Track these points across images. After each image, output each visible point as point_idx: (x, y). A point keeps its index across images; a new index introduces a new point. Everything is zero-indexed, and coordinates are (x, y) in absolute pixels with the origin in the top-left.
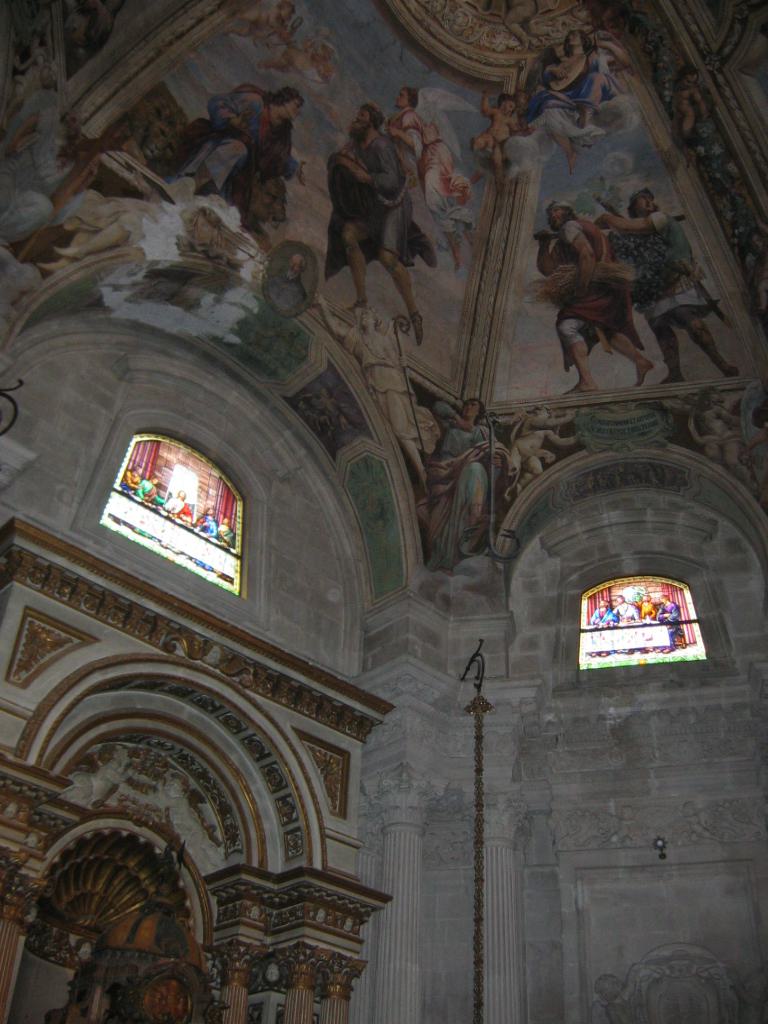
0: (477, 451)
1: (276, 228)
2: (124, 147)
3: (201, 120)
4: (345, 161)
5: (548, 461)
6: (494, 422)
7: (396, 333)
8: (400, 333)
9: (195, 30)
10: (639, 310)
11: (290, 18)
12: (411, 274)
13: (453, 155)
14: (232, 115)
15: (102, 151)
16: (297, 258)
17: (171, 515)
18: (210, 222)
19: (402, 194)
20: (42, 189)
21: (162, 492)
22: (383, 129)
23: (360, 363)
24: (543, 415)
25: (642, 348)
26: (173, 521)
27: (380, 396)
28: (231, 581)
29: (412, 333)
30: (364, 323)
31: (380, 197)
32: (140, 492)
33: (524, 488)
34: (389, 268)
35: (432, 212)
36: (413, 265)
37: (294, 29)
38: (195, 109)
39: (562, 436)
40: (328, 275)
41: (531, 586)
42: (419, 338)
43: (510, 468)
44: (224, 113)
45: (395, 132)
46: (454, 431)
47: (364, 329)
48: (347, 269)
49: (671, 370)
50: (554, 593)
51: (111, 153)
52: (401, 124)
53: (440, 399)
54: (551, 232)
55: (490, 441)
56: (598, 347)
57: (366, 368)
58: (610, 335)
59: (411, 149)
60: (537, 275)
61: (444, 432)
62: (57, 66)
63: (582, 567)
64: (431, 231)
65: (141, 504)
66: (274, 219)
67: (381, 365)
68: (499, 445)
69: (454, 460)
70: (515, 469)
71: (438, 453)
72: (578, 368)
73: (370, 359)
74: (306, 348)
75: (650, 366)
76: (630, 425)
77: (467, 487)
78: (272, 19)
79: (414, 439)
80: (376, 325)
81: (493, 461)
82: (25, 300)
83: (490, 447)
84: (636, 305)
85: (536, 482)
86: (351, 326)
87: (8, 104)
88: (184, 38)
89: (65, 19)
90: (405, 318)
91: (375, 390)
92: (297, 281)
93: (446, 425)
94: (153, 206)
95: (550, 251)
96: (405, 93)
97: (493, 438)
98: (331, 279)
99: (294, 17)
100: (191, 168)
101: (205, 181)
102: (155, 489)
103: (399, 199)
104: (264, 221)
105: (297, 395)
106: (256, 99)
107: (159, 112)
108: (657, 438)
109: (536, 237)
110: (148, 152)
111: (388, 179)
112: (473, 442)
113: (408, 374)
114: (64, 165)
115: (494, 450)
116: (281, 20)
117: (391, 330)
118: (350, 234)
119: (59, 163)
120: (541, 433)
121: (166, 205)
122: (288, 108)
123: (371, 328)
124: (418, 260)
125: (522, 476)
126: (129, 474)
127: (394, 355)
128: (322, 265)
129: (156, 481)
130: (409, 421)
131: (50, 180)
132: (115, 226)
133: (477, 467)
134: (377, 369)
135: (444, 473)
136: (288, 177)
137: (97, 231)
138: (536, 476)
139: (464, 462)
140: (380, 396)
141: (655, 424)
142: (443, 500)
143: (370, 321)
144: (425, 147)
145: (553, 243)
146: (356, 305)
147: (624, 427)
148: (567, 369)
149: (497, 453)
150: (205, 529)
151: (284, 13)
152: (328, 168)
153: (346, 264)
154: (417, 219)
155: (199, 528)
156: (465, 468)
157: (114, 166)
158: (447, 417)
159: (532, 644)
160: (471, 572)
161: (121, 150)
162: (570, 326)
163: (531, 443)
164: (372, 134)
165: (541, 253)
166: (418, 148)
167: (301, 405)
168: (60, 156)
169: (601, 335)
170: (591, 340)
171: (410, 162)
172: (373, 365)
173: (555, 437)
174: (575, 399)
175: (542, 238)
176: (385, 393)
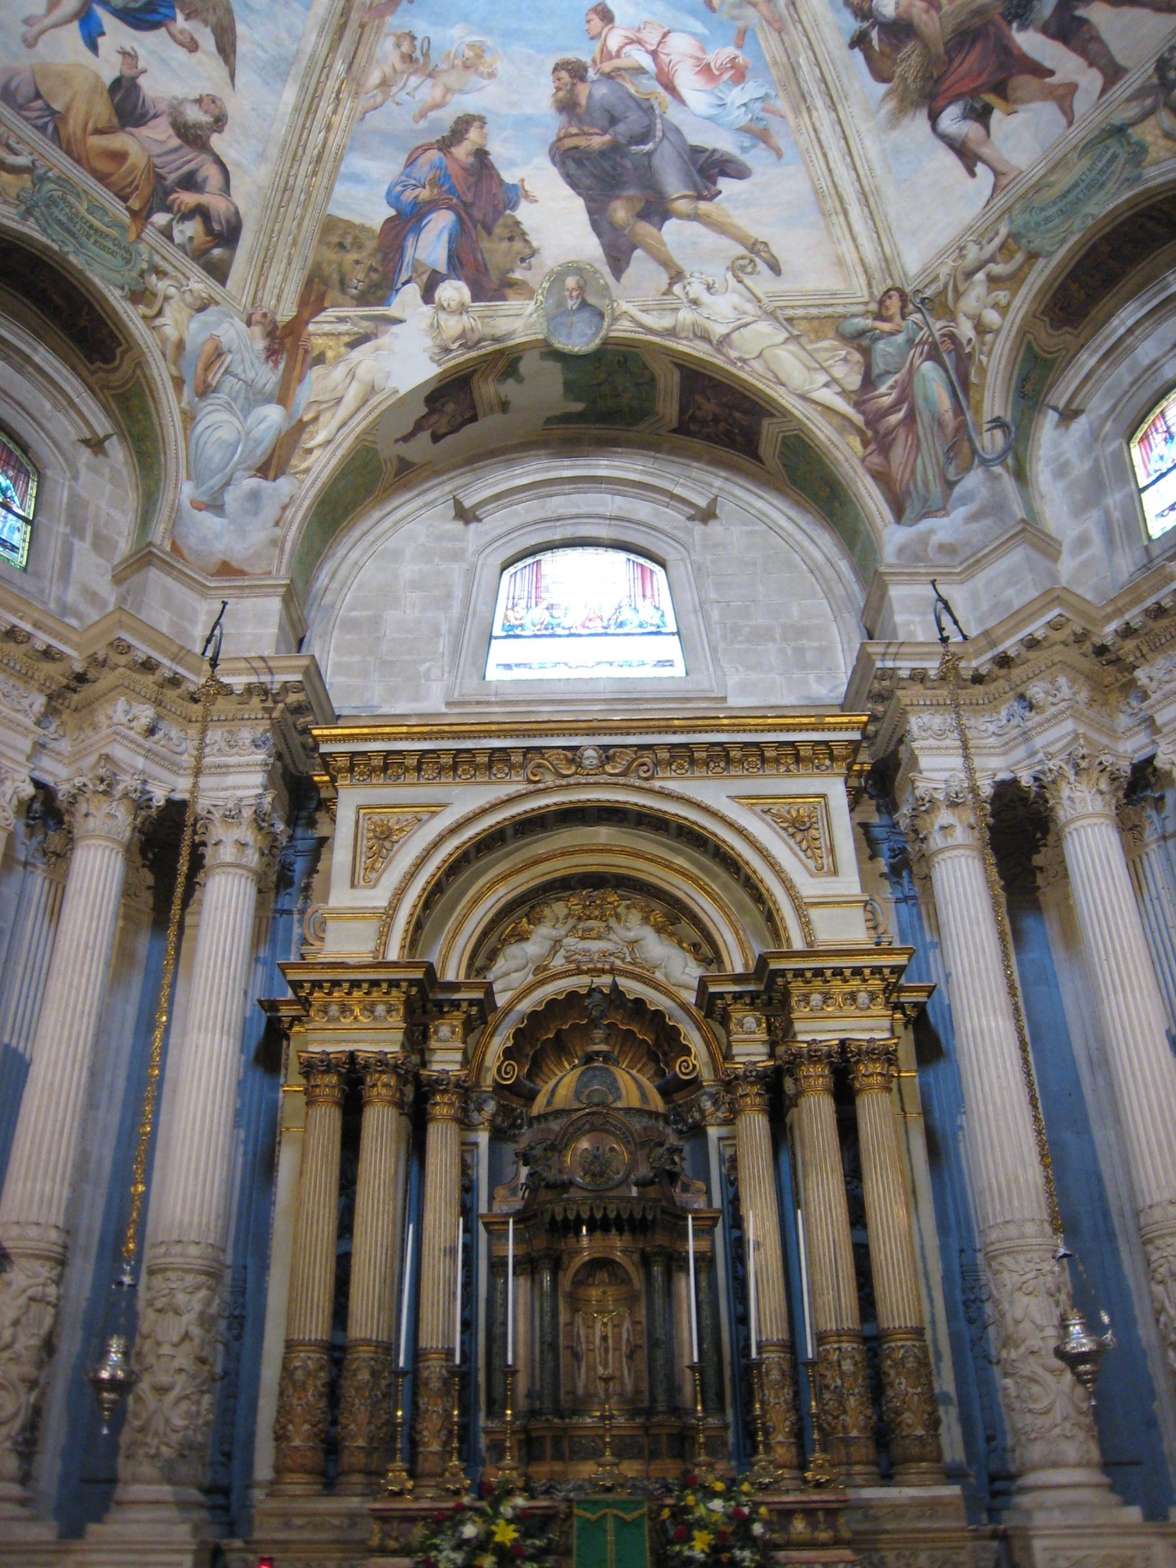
0: (919, 349)
1: (529, 268)
2: (326, 304)
3: (389, 221)
4: (569, 143)
5: (1003, 302)
6: (923, 300)
7: (740, 282)
8: (748, 281)
9: (330, 142)
10: (1023, 27)
11: (414, 47)
12: (726, 205)
13: (694, 35)
14: (417, 191)
15: (307, 323)
16: (571, 282)
17: (573, 631)
18: (453, 312)
19: (659, 126)
20: (268, 400)
21: (555, 613)
22: (591, 74)
23: (709, 341)
24: (973, 254)
25: (1051, 73)
26: (580, 635)
27: (754, 363)
28: (670, 663)
29: (761, 266)
30: (691, 296)
31: (634, 148)
32: (528, 625)
33: (989, 355)
34: (695, 217)
35: (709, 118)
36: (720, 192)
37: (426, 55)
38: (377, 214)
39: (1006, 262)
40: (618, 279)
41: (1061, 471)
42: (775, 267)
43: (964, 342)
44: (409, 195)
45: (607, 67)
46: (880, 345)
47: (695, 302)
48: (638, 253)
49: (1102, 70)
50: (1087, 465)
51: (317, 319)
52: (609, 53)
53: (844, 317)
54: (866, 25)
55: (928, 324)
56: (997, 116)
57: (720, 343)
58: (1000, 89)
59: (640, 71)
60: (882, 88)
61: (866, 352)
62: (199, 284)
63: (1114, 407)
64: (724, 143)
65: (535, 636)
66: (523, 260)
67: (739, 328)
68: (939, 324)
69: (897, 376)
70: (970, 340)
71: (869, 381)
72: (984, 162)
73: (719, 330)
74: (645, 367)
75: (1073, 88)
76: (1083, 185)
77: (926, 399)
78: (399, 66)
79: (826, 385)
80: (709, 288)
81: (942, 348)
82: (289, 513)
83: (931, 334)
84: (1015, 25)
85: (1002, 337)
86: (678, 309)
87: (164, 355)
88: (325, 157)
89: (170, 238)
90: (742, 258)
91: (744, 361)
92: (584, 305)
93: (865, 342)
94: (383, 340)
95: (877, 48)
96: (593, 16)
97: (930, 320)
98: (625, 278)
99: (418, 43)
100: (404, 277)
101: (425, 277)
102: (547, 613)
103: (659, 134)
104: (512, 270)
105: (680, 420)
106: (434, 155)
107: (341, 246)
108: (1125, 175)
109: (853, 45)
110: (354, 292)
111: (633, 122)
112: (910, 342)
113: (781, 317)
114: (276, 363)
115: (937, 335)
116: (409, 58)
117: (732, 281)
118: (620, 212)
119: (271, 364)
120: (980, 276)
121: (395, 329)
122: (473, 134)
123: (705, 297)
124: (724, 184)
125: (983, 343)
126: (510, 613)
127: (750, 308)
128: (605, 270)
129: (544, 604)
130: (809, 369)
131: (269, 387)
132: (355, 384)
133: (928, 367)
134: (735, 336)
135: (887, 401)
136: (514, 207)
137: (339, 401)
138: (997, 332)
139: (911, 371)
140: (754, 363)
141: (1115, 157)
142: (901, 434)
143: (696, 289)
144: (654, 54)
145: (874, 34)
146: (671, 285)
147: (1078, 190)
148: (972, 174)
149: (943, 335)
150: (621, 625)
151: (405, 48)
152: (554, 163)
153: (634, 247)
154: (694, 140)
155: (614, 629)
156: (915, 379)
157: (327, 328)
158: (862, 333)
159: (1083, 542)
160: (964, 500)
161: (324, 309)
162: (951, 120)
163: (975, 296)
164: (583, 91)
165: (869, 59)
166: (646, 62)
167: (693, 427)
168: (268, 358)
169: (990, 98)
170: (982, 115)
171: (650, 86)
172: (728, 335)
173: (997, 269)
174: (1001, 201)
175: (859, 41)
176: (760, 355)
